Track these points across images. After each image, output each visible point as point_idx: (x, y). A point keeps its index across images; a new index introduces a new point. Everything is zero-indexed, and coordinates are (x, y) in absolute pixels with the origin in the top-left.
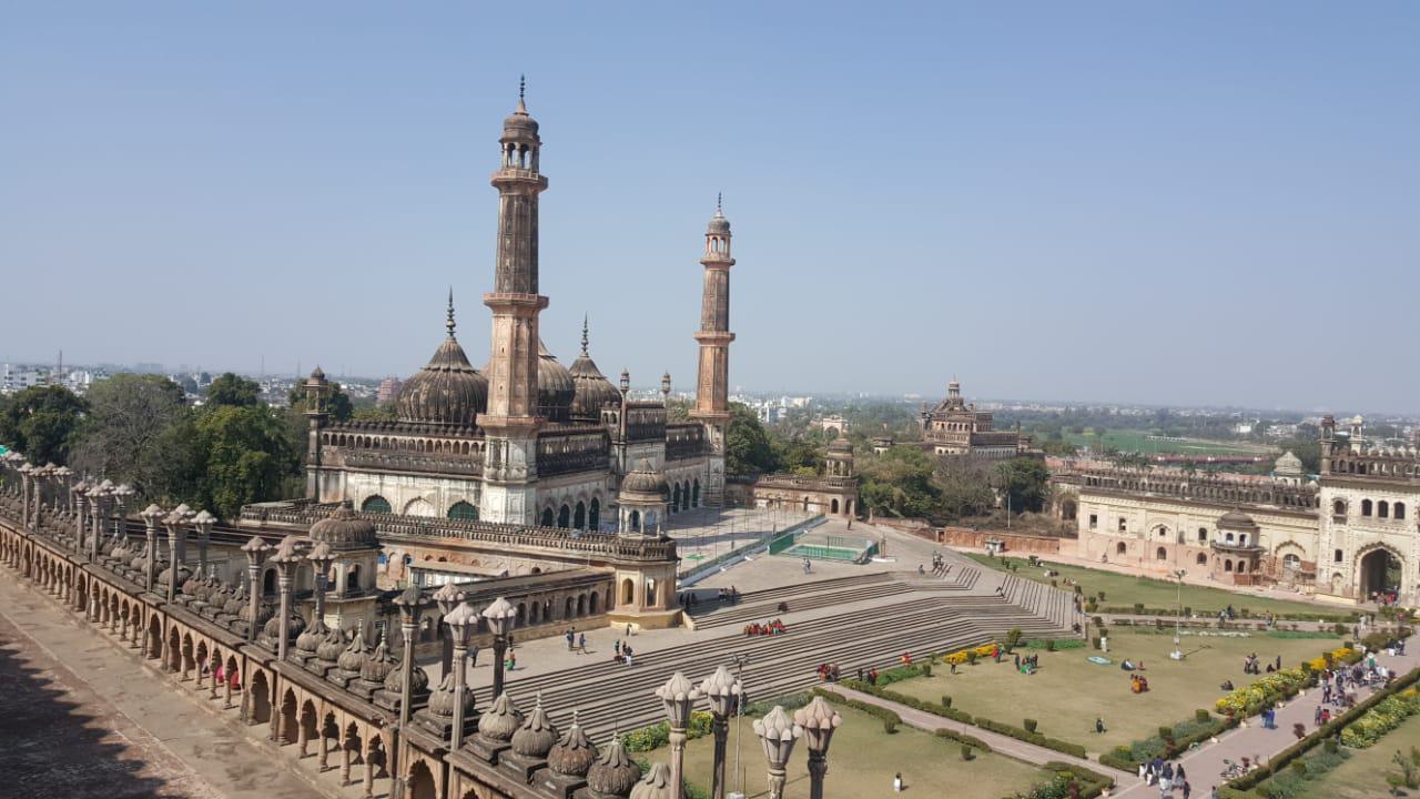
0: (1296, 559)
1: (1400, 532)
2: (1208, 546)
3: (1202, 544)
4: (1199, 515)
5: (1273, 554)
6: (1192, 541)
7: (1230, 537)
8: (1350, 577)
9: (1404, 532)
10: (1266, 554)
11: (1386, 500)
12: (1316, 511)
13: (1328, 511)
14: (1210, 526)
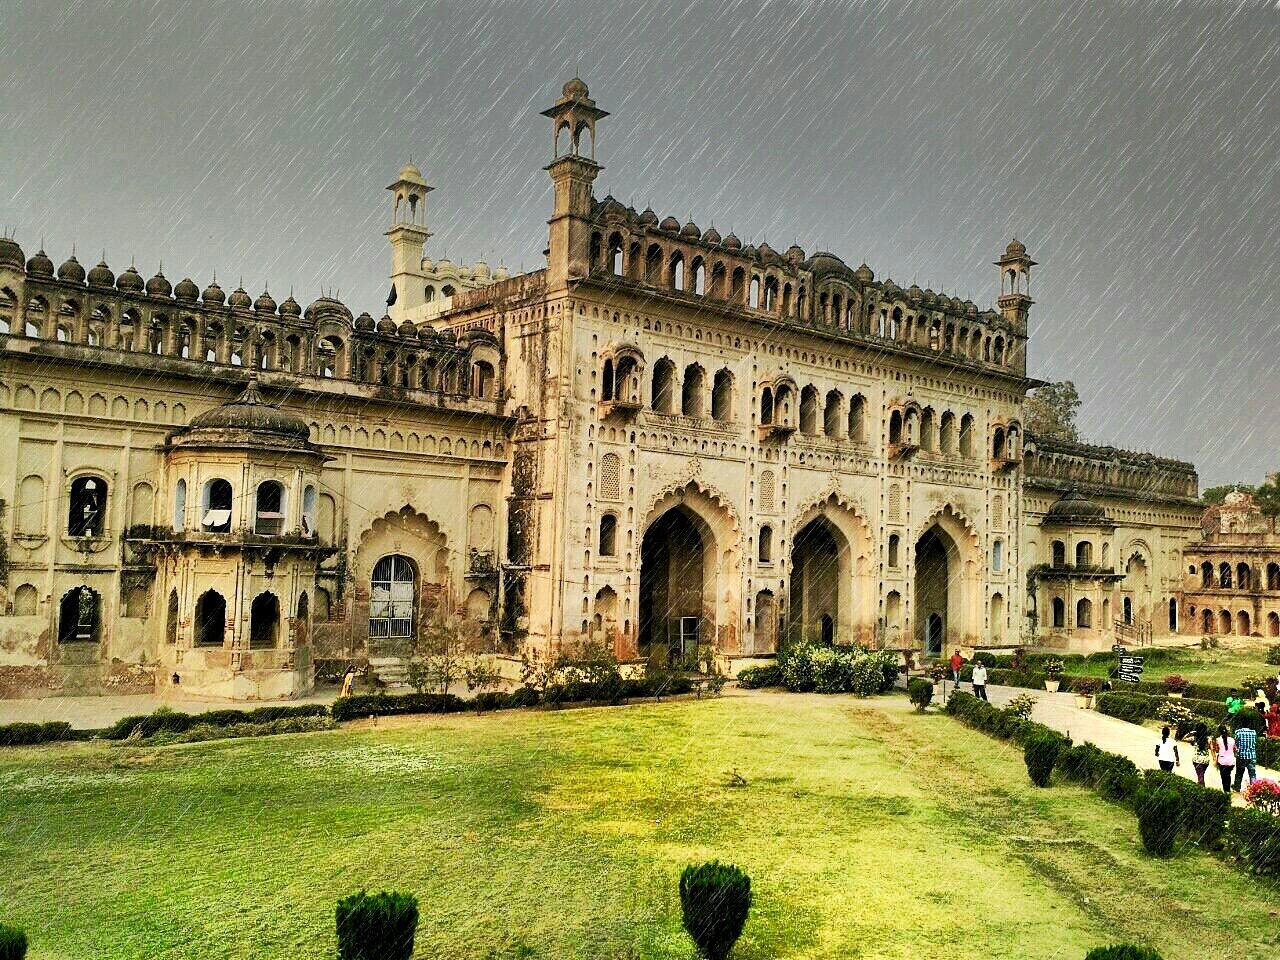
0: (404, 567)
1: (729, 452)
2: (112, 556)
3: (86, 548)
4: (70, 421)
5: (351, 559)
6: (43, 539)
7: (269, 496)
8: (635, 595)
9: (738, 453)
10: (331, 562)
11: (702, 362)
12: (473, 406)
13: (587, 394)
14: (117, 460)
